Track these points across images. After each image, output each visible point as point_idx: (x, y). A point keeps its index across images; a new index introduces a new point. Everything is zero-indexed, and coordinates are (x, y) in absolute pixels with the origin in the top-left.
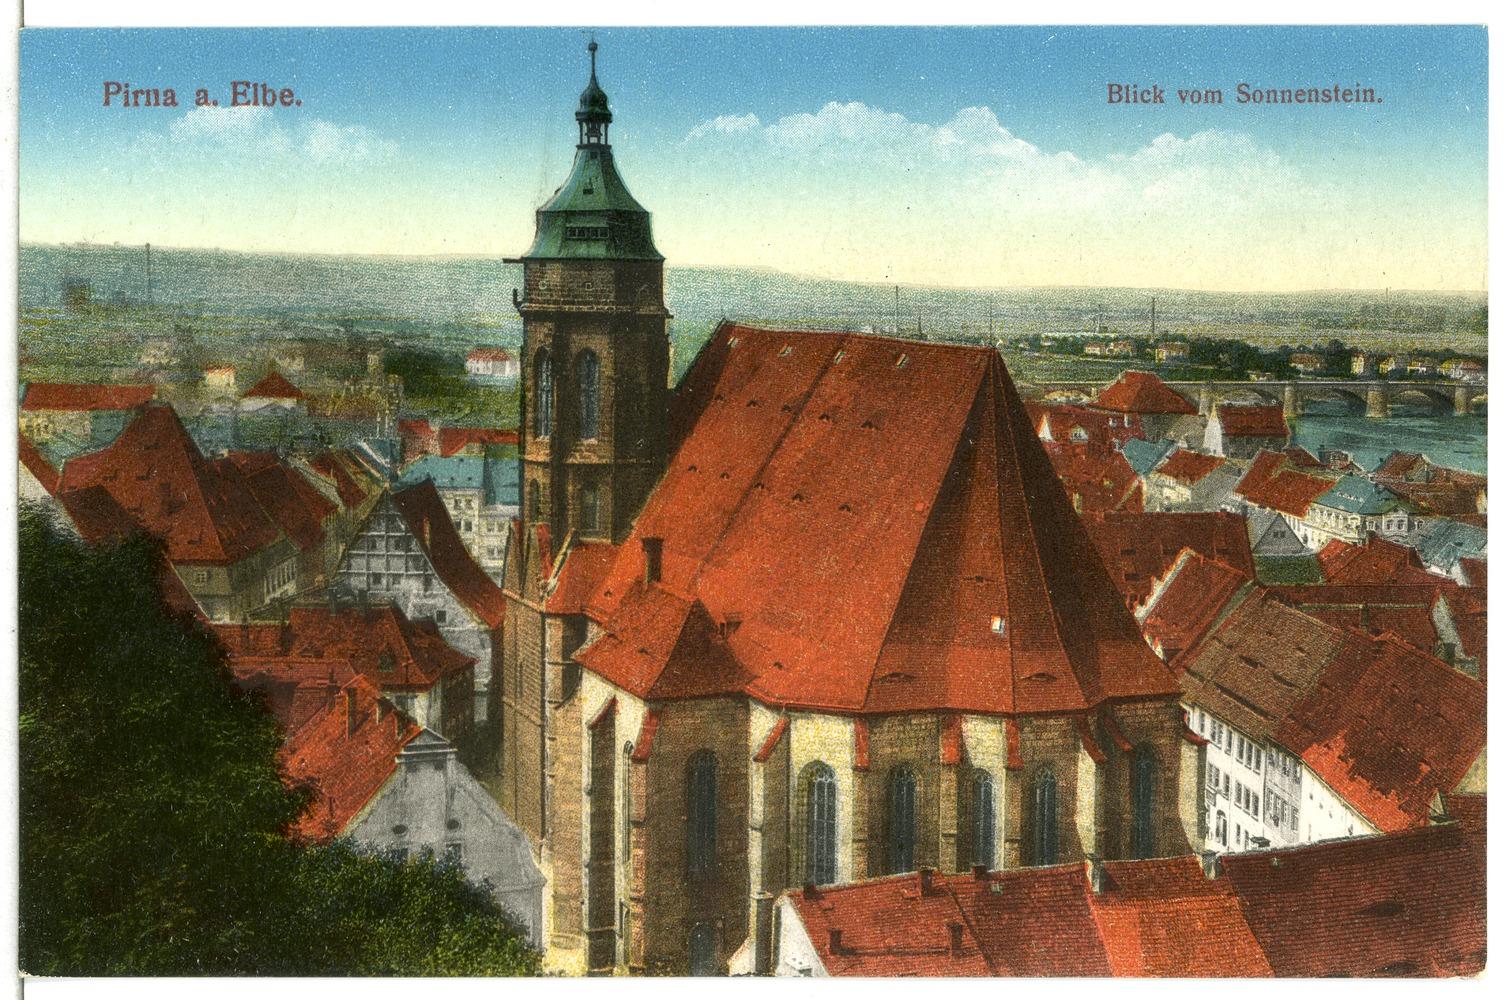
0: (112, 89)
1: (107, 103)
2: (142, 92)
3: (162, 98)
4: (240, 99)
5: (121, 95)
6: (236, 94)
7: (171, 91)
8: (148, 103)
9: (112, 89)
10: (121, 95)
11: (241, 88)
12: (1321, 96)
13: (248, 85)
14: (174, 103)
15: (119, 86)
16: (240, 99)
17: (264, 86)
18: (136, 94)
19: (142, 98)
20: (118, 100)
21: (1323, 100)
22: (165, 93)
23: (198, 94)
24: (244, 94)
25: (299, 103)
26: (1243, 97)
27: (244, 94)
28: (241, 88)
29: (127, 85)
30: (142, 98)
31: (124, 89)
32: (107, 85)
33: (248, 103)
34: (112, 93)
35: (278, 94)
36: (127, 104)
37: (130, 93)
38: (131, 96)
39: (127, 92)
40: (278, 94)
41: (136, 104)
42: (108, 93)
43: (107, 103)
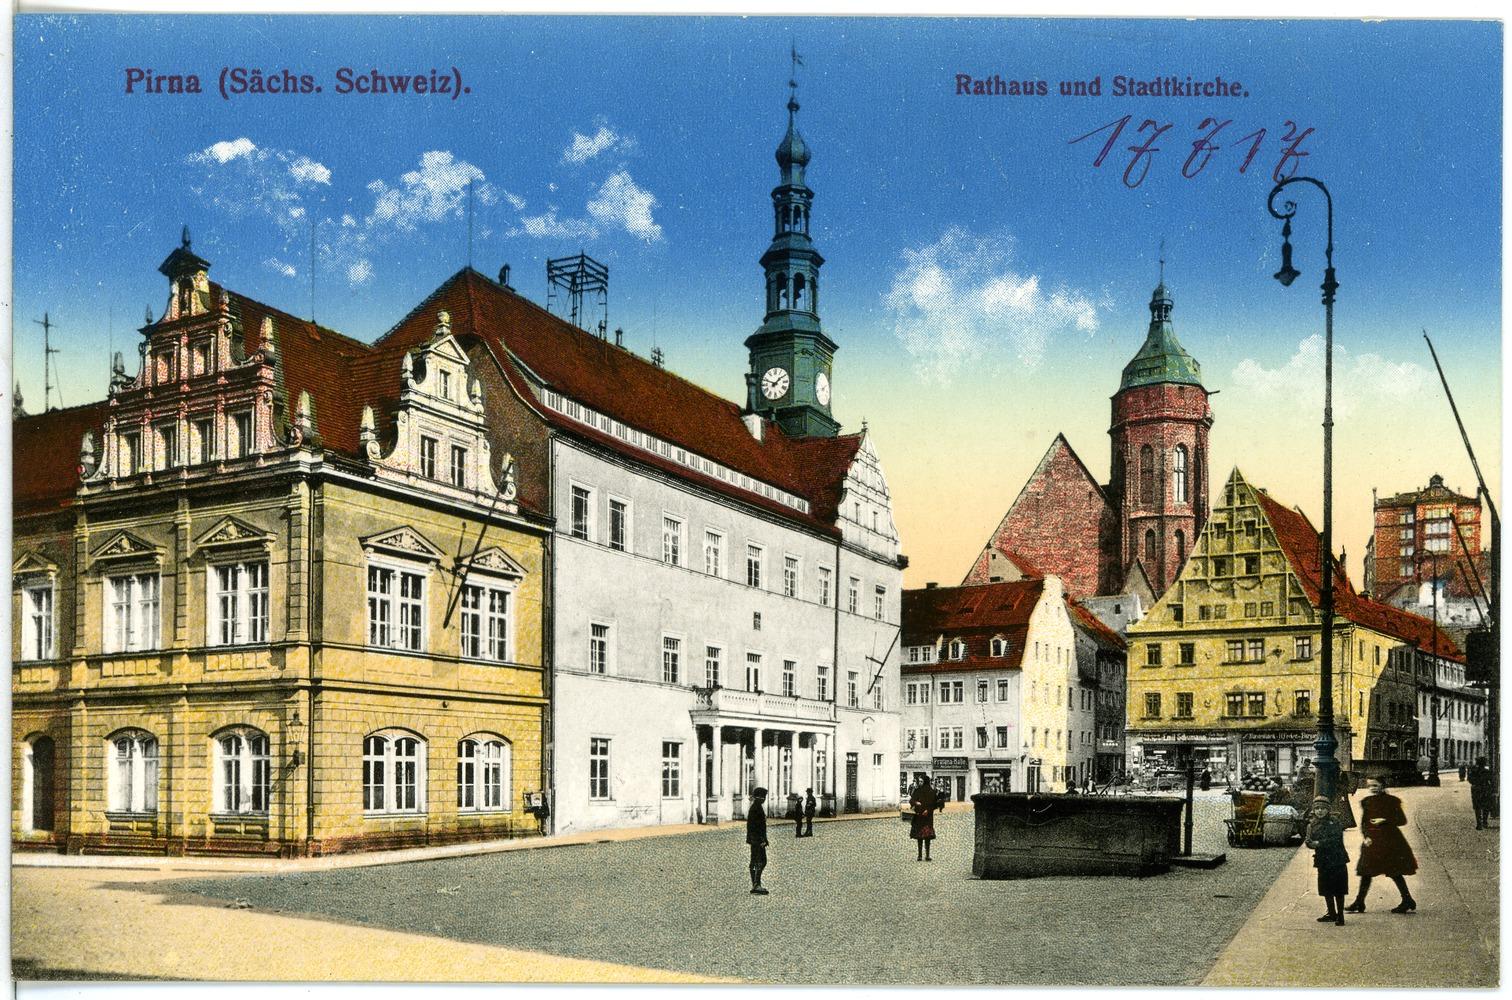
0: (135, 75)
1: (129, 90)
2: (164, 78)
3: (185, 85)
5: (144, 82)
7: (195, 78)
8: (171, 90)
9: (135, 75)
10: (144, 82)
12: (299, 84)
14: (197, 90)
15: (142, 73)
18: (159, 79)
20: (140, 87)
21: (303, 90)
22: (189, 80)
26: (345, 86)
29: (149, 72)
30: (165, 84)
31: (146, 75)
32: (129, 72)
34: (136, 80)
36: (149, 90)
37: (153, 79)
38: (154, 86)
39: (149, 79)
42: (130, 81)
43: (129, 90)
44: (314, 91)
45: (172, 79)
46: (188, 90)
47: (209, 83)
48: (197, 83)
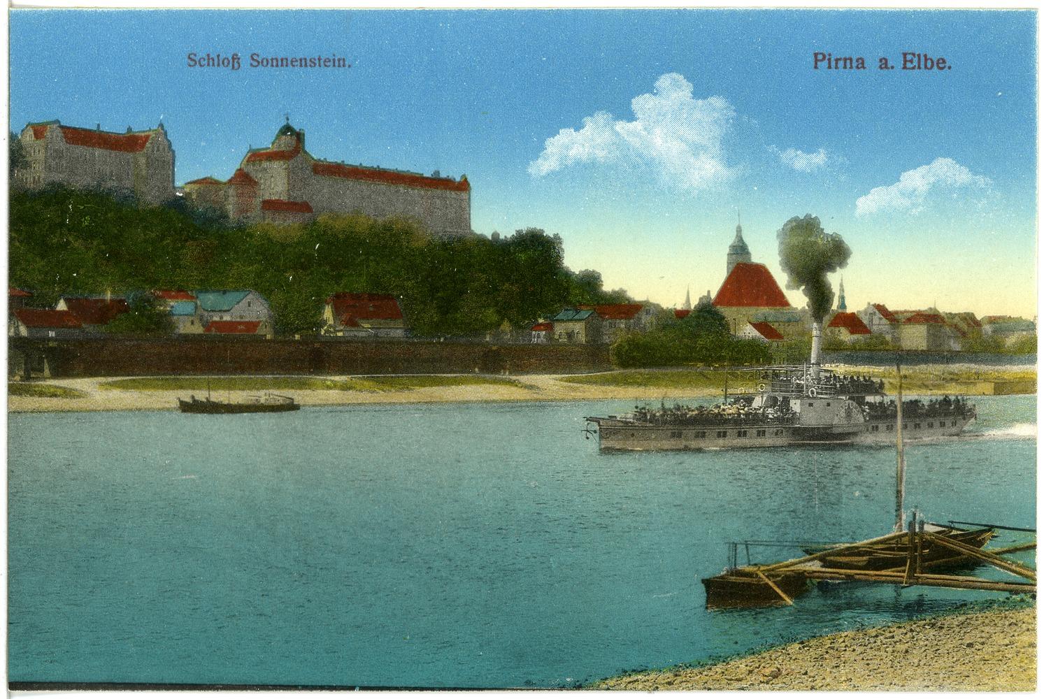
2: (840, 59)
3: (854, 64)
4: (909, 65)
6: (905, 61)
7: (861, 58)
9: (820, 57)
11: (909, 57)
13: (914, 55)
14: (864, 68)
16: (909, 65)
17: (925, 56)
18: (837, 60)
19: (841, 64)
23: (881, 60)
24: (911, 61)
25: (950, 68)
27: (911, 61)
28: (909, 57)
29: (830, 55)
30: (841, 64)
32: (816, 55)
33: (913, 68)
34: (821, 61)
35: (935, 60)
36: (830, 67)
38: (833, 64)
39: (829, 60)
40: (935, 60)
41: (836, 67)
42: (816, 61)
44: (946, 69)
45: (845, 60)
46: (857, 67)
47: (872, 63)
48: (863, 63)
